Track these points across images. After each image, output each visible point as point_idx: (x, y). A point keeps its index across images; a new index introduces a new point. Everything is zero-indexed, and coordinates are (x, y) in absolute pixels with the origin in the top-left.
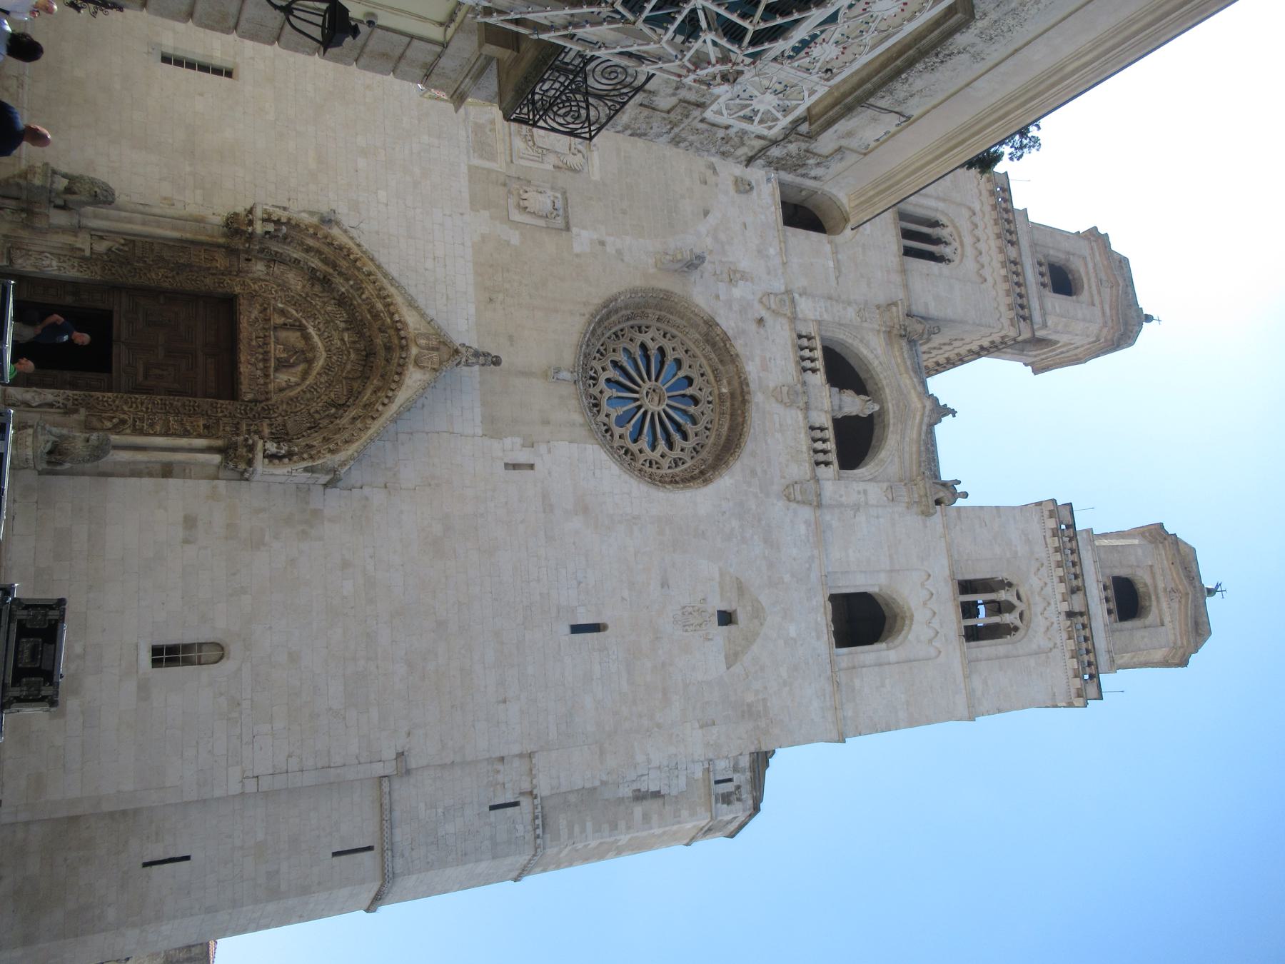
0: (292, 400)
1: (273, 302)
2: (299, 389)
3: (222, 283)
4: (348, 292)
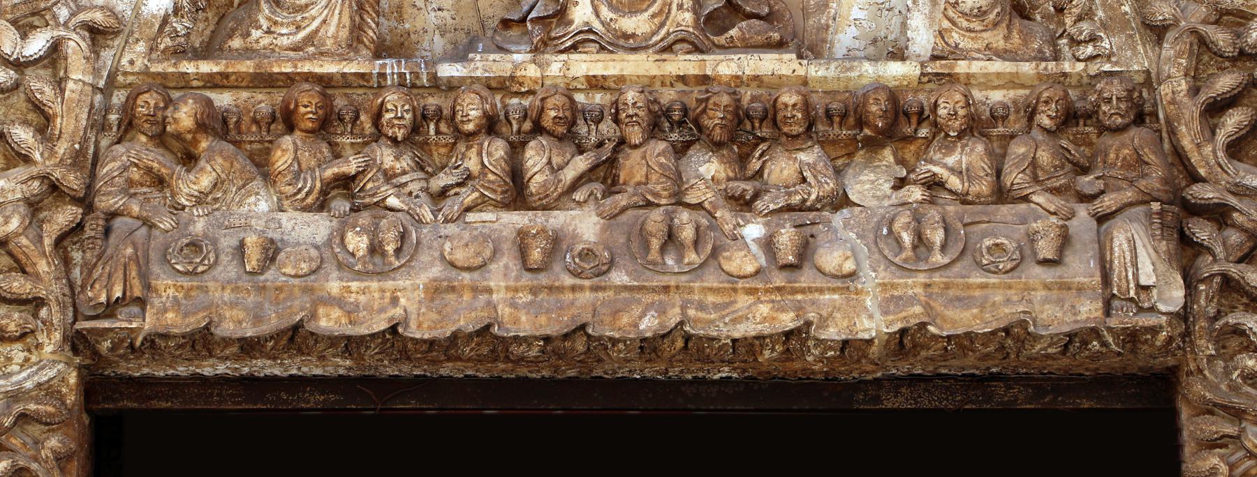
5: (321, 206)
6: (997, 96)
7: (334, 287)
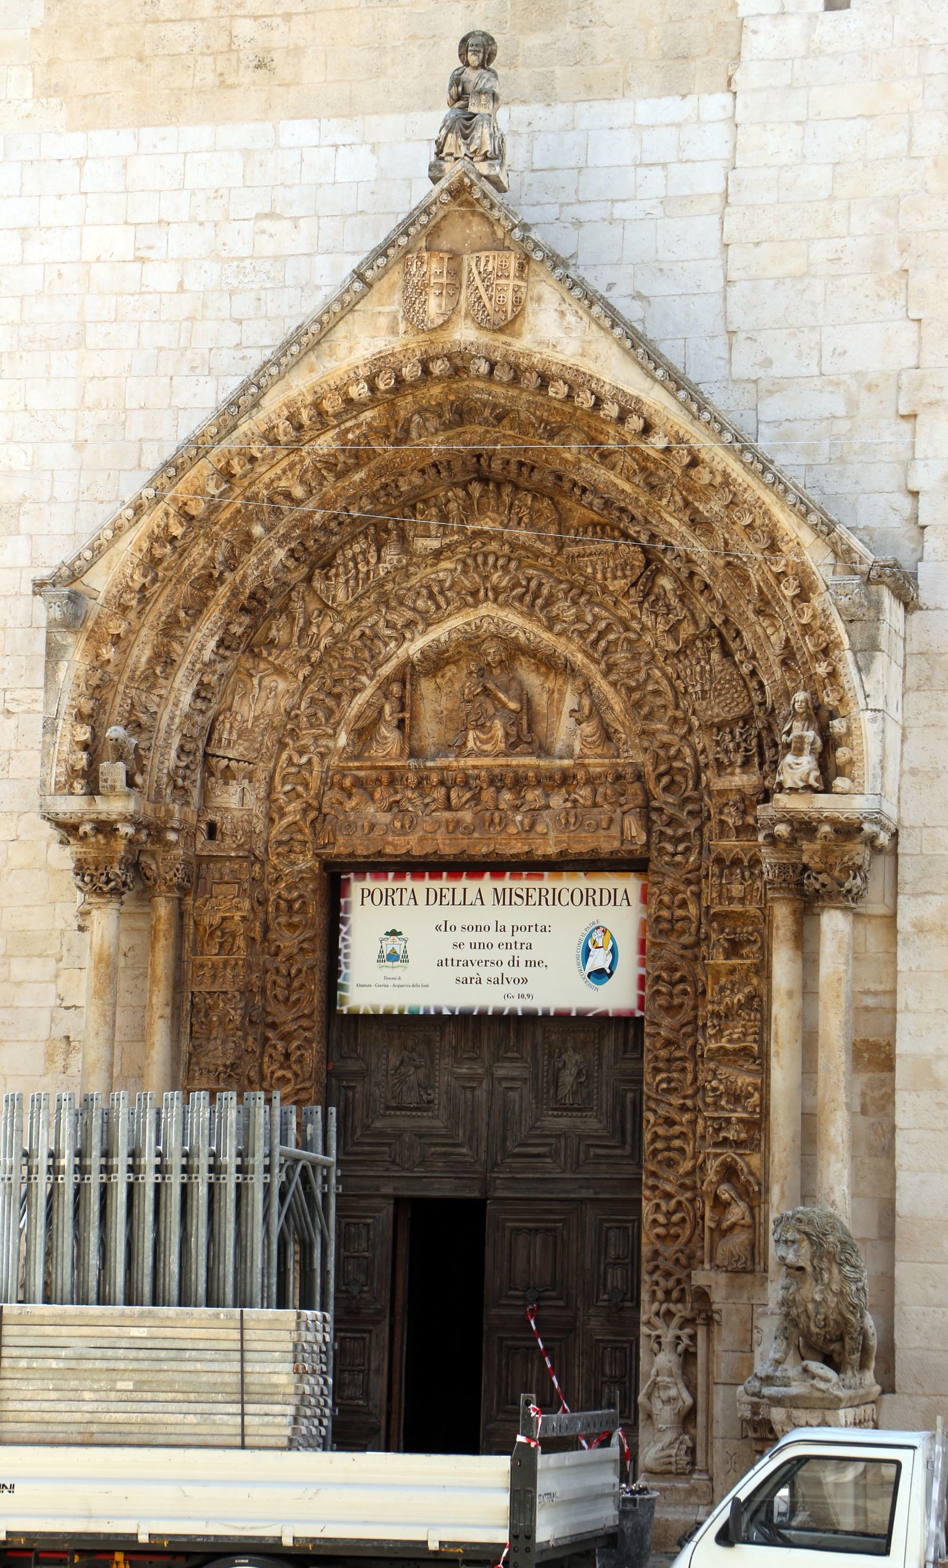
0: (638, 705)
1: (334, 761)
2: (602, 684)
3: (290, 903)
4: (286, 537)
5: (390, 809)
6: (598, 770)
7: (390, 839)
